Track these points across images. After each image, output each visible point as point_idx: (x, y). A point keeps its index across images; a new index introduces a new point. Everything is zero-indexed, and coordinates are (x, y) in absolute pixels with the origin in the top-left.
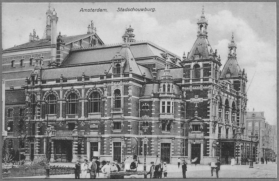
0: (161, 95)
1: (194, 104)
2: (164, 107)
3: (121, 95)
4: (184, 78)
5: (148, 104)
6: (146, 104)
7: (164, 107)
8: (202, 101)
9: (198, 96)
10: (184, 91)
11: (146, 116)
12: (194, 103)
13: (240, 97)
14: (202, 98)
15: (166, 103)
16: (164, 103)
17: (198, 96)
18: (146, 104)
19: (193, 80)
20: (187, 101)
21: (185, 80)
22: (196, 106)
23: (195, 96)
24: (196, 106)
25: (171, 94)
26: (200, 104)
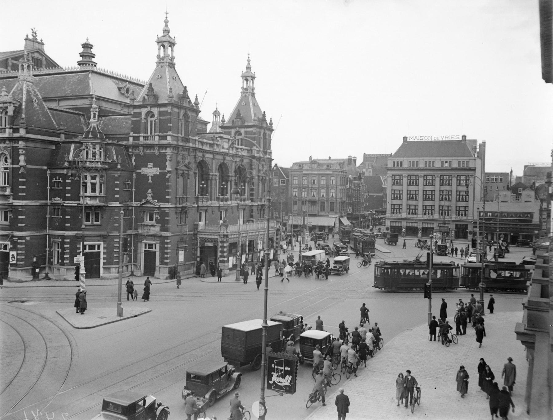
1: (146, 177)
3: (9, 163)
4: (131, 134)
6: (57, 178)
8: (158, 174)
9: (152, 164)
10: (132, 155)
11: (57, 198)
13: (254, 157)
15: (89, 178)
16: (86, 177)
17: (152, 164)
18: (57, 178)
19: (144, 137)
21: (133, 137)
22: (150, 181)
24: (150, 181)
25: (97, 162)
26: (154, 177)
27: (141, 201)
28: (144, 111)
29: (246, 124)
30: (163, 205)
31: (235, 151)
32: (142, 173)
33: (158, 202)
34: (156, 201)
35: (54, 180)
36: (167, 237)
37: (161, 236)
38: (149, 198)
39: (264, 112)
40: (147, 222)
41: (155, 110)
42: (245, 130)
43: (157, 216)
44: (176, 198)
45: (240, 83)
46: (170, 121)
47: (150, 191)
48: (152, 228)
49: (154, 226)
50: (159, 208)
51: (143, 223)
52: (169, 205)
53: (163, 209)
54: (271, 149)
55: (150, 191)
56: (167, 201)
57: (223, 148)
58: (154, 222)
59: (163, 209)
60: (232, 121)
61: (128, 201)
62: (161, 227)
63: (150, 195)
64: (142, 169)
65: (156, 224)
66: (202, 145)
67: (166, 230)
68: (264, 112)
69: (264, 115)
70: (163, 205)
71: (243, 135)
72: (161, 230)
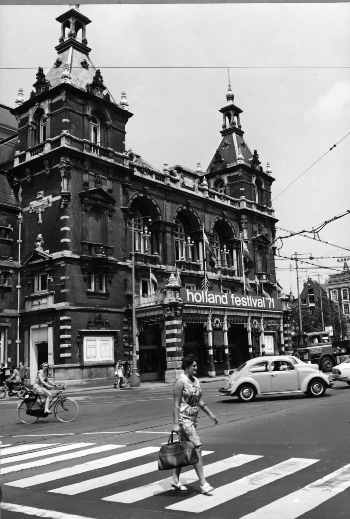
9: (42, 192)
14: (51, 196)
28: (31, 112)
29: (229, 166)
30: (56, 255)
31: (207, 195)
32: (31, 212)
34: (48, 251)
36: (63, 312)
38: (39, 249)
39: (255, 152)
40: (38, 291)
42: (228, 175)
44: (83, 244)
45: (219, 121)
47: (40, 236)
48: (44, 301)
51: (33, 295)
54: (274, 206)
55: (40, 236)
56: (65, 246)
57: (183, 186)
60: (211, 168)
61: (7, 259)
64: (31, 203)
66: (142, 173)
68: (255, 152)
69: (256, 156)
70: (56, 255)
71: (226, 182)
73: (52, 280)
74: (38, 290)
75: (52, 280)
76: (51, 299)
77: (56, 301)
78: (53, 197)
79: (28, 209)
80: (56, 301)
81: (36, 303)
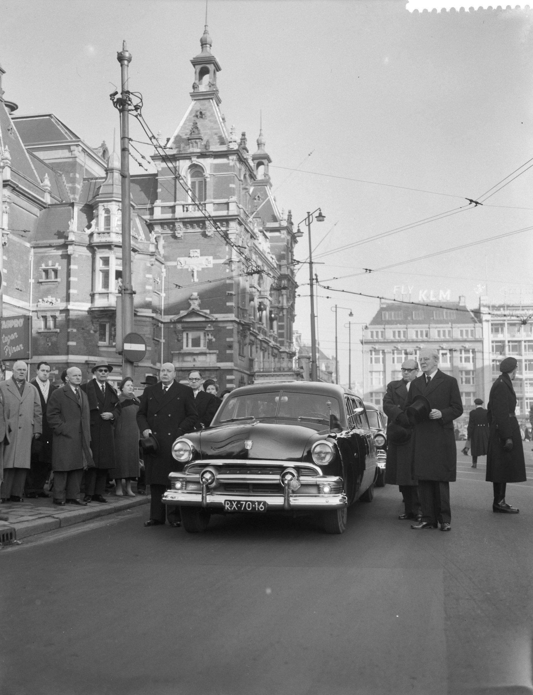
0: (96, 239)
2: (106, 274)
5: (57, 264)
6: (50, 263)
7: (106, 274)
8: (211, 266)
9: (198, 251)
12: (187, 269)
16: (106, 261)
17: (198, 251)
18: (50, 263)
20: (169, 264)
23: (191, 250)
27: (178, 313)
30: (220, 317)
32: (179, 267)
33: (212, 312)
34: (208, 311)
35: (43, 266)
36: (230, 371)
37: (218, 369)
41: (207, 163)
43: (210, 337)
46: (230, 180)
49: (205, 354)
50: (216, 321)
51: (182, 351)
52: (232, 317)
53: (221, 325)
56: (229, 310)
58: (202, 348)
59: (221, 325)
62: (218, 355)
63: (197, 302)
64: (178, 259)
65: (208, 351)
67: (230, 359)
70: (220, 317)
72: (220, 360)
73: (214, 340)
74: (187, 346)
75: (214, 340)
76: (214, 358)
77: (220, 360)
78: (214, 258)
79: (173, 263)
80: (220, 359)
81: (189, 358)
